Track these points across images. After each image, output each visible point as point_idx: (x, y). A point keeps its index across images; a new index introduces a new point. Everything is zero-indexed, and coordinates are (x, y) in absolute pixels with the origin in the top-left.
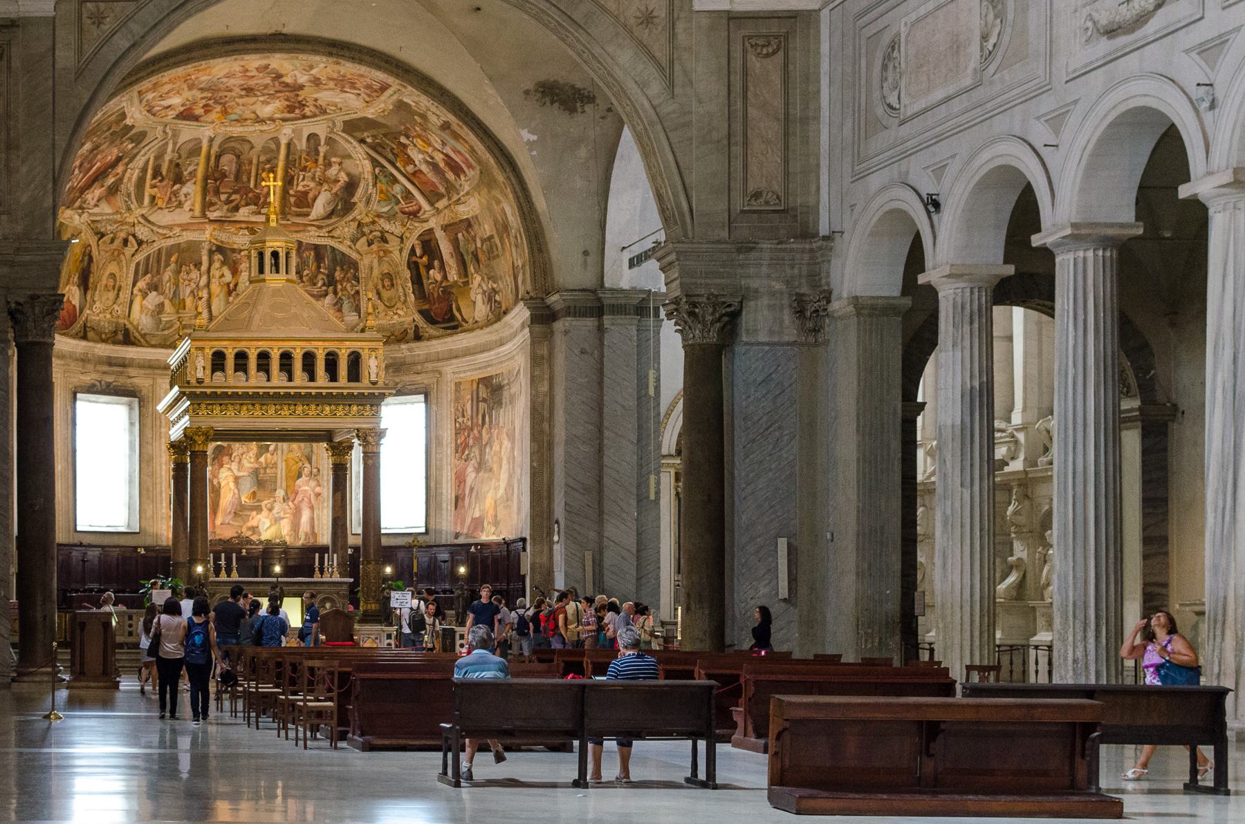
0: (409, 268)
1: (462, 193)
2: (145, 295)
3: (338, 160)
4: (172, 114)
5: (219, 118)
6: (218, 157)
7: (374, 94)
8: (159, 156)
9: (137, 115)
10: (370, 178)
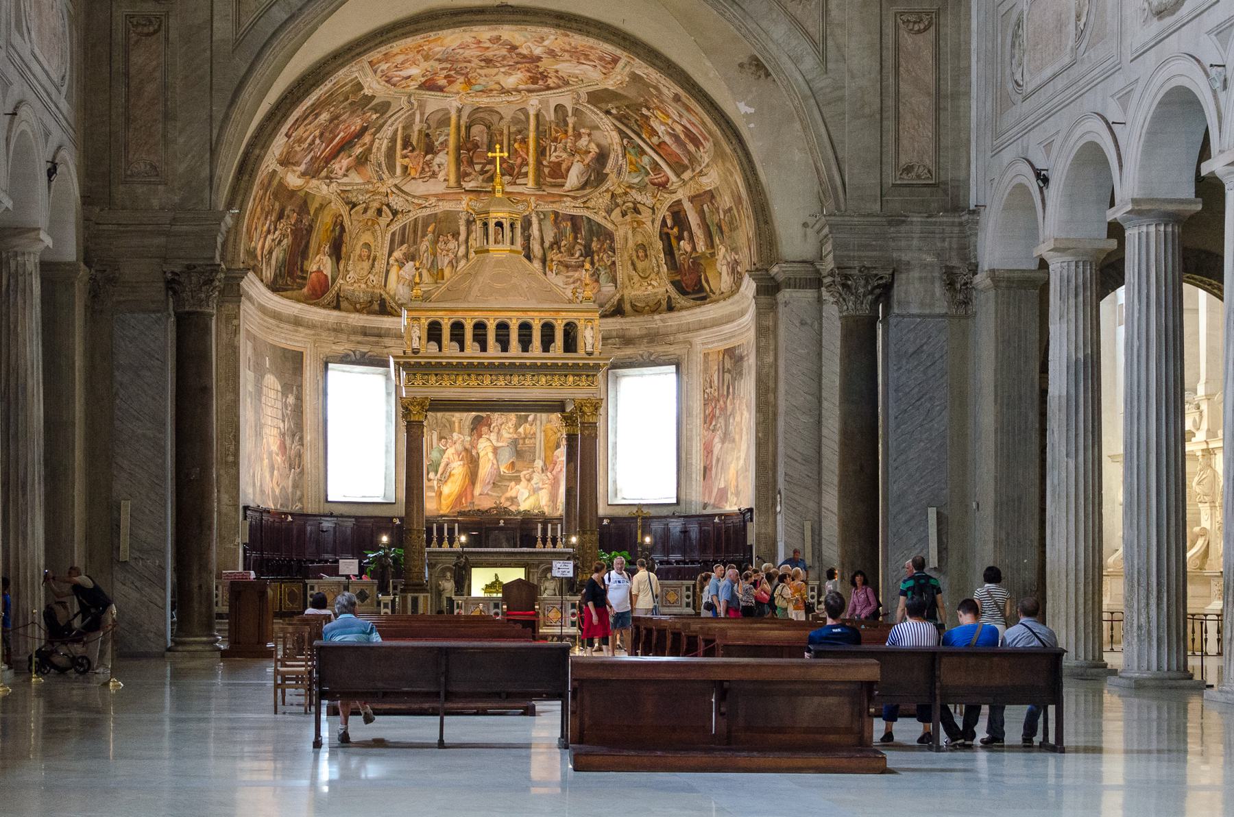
2: (401, 265)
3: (588, 131)
4: (413, 85)
6: (468, 128)
8: (407, 127)
9: (375, 85)
10: (619, 149)
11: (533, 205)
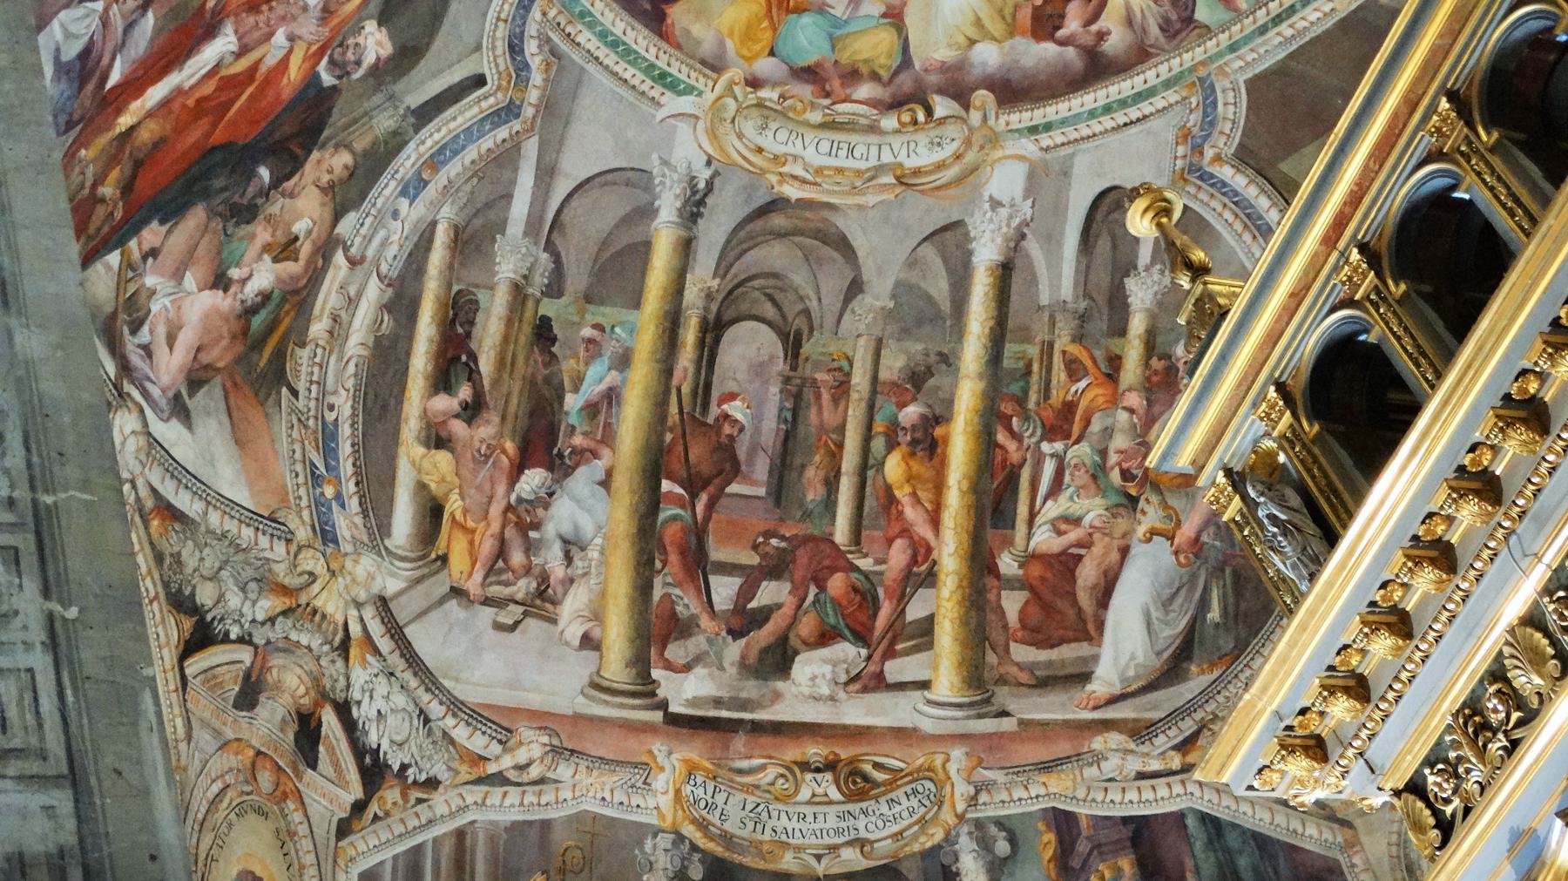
5: (748, 36)
11: (962, 789)
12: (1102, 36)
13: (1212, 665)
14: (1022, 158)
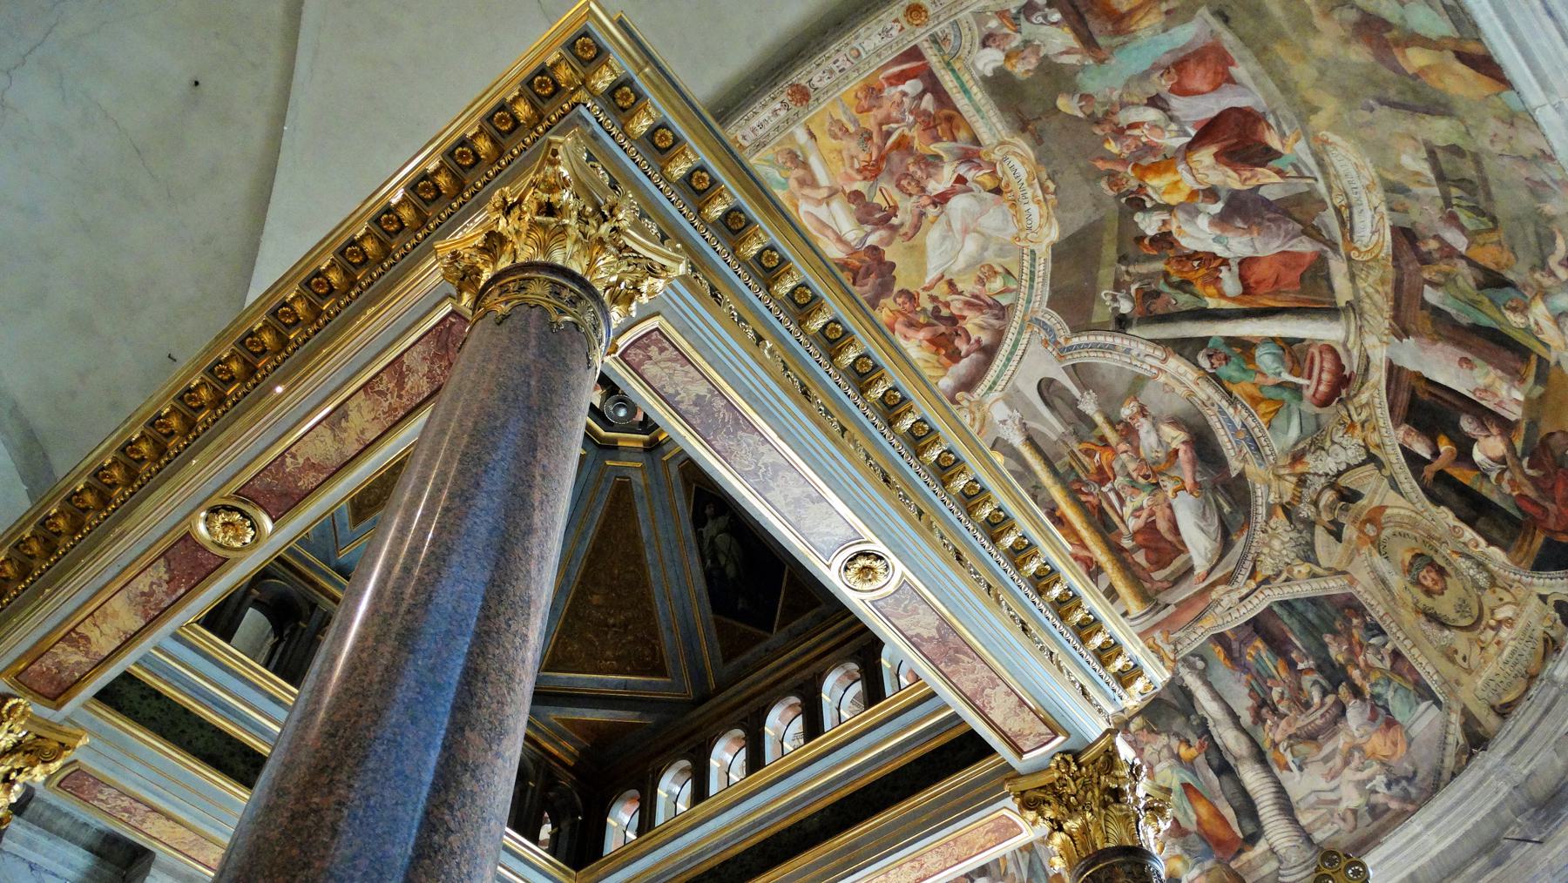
0: (1437, 501)
1: (1321, 187)
7: (962, 135)
10: (1210, 391)
12: (978, 341)
13: (1242, 531)
14: (997, 400)
